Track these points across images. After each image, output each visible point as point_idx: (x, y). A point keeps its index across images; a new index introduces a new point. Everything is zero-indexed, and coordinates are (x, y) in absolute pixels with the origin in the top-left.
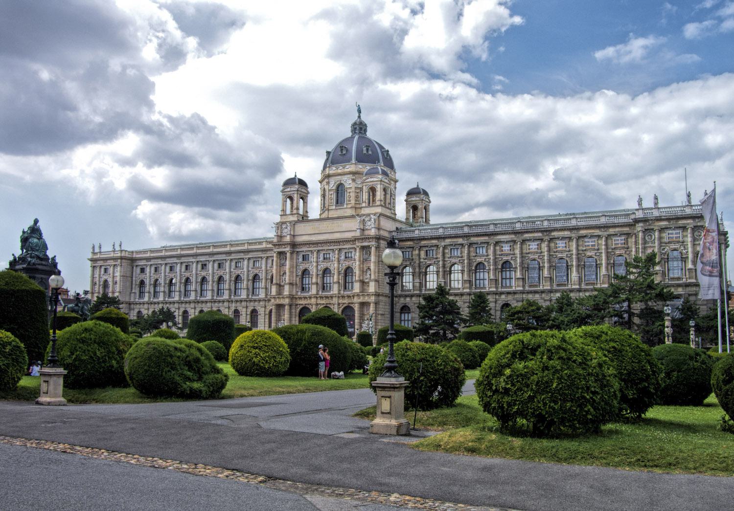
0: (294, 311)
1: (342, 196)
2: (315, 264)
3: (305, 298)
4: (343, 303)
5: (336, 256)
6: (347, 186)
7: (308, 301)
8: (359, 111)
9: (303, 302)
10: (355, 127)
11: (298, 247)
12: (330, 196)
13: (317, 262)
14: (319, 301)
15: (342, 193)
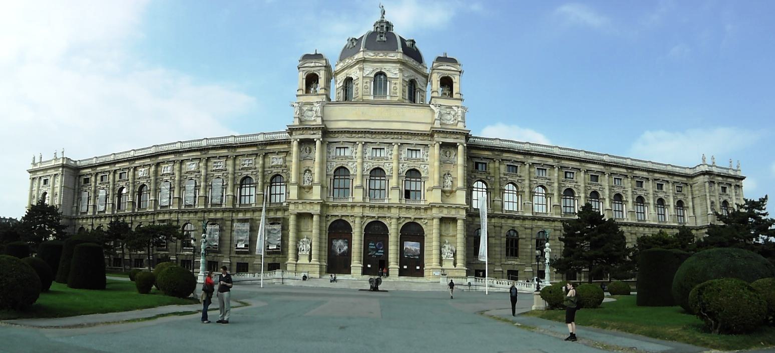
0: (324, 224)
1: (380, 87)
2: (359, 161)
3: (343, 206)
4: (406, 218)
5: (395, 152)
6: (389, 75)
7: (348, 212)
8: (384, 13)
9: (339, 212)
10: (382, 24)
11: (331, 135)
12: (365, 84)
13: (363, 158)
14: (368, 212)
15: (381, 84)
